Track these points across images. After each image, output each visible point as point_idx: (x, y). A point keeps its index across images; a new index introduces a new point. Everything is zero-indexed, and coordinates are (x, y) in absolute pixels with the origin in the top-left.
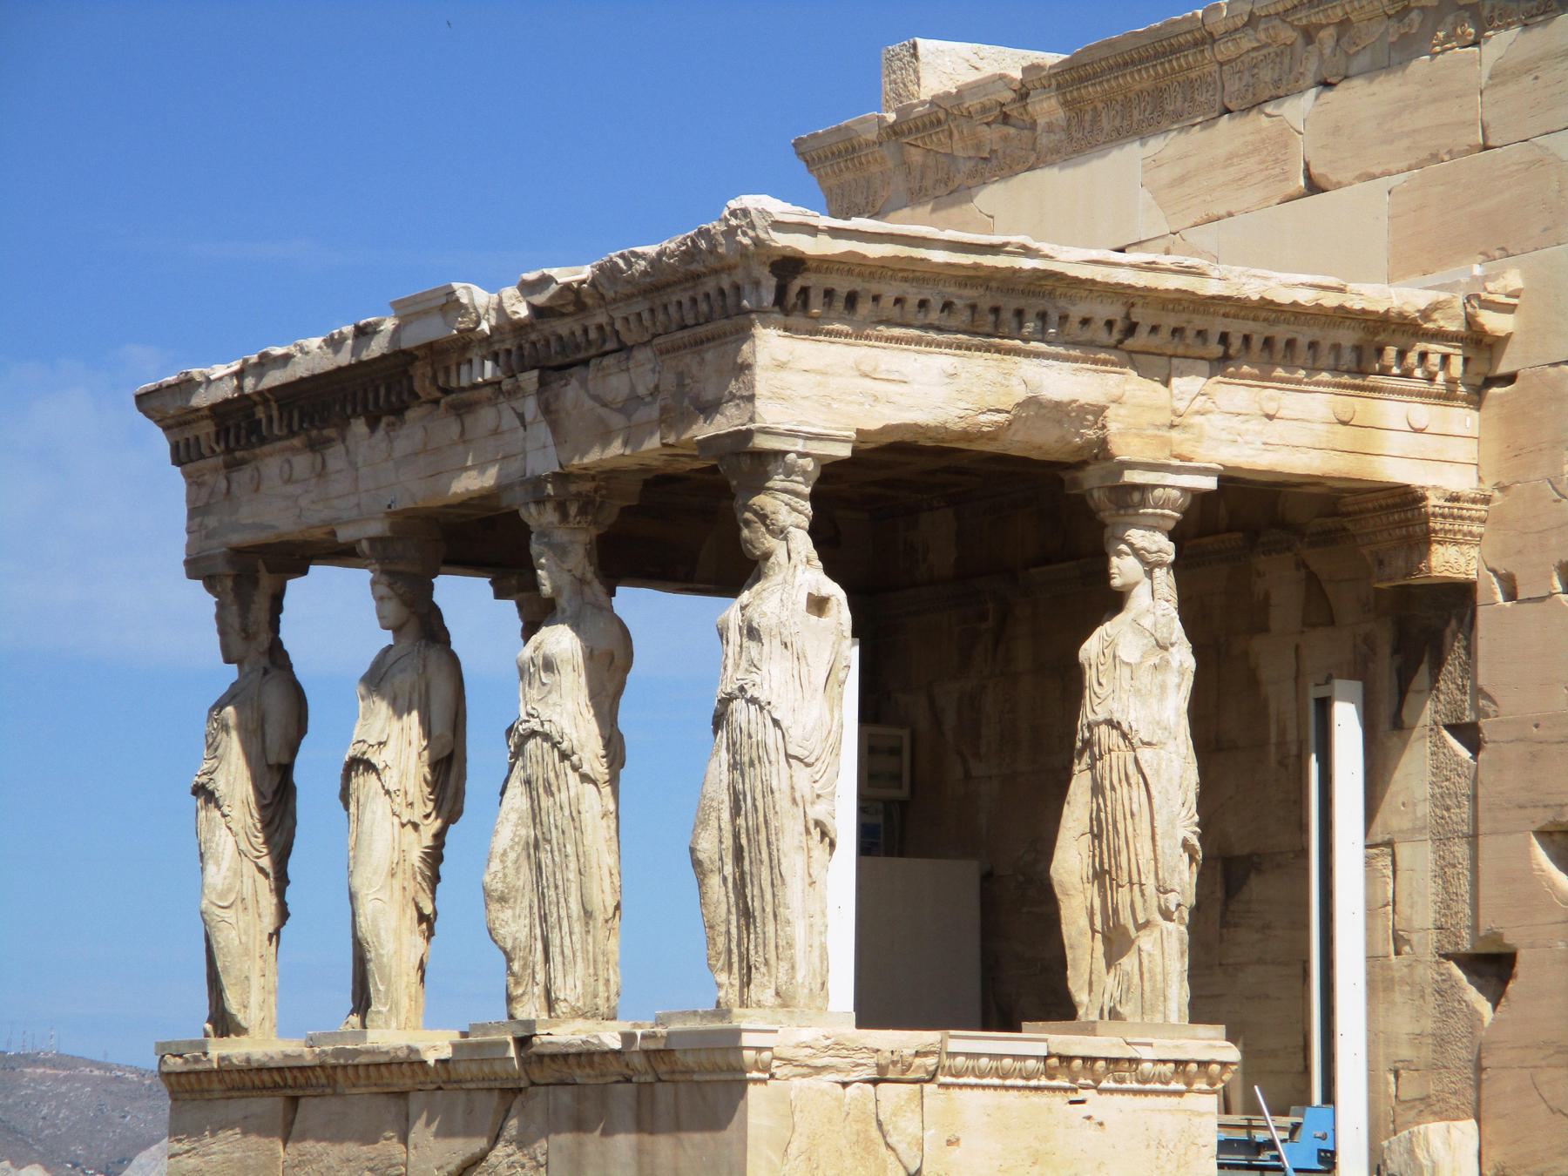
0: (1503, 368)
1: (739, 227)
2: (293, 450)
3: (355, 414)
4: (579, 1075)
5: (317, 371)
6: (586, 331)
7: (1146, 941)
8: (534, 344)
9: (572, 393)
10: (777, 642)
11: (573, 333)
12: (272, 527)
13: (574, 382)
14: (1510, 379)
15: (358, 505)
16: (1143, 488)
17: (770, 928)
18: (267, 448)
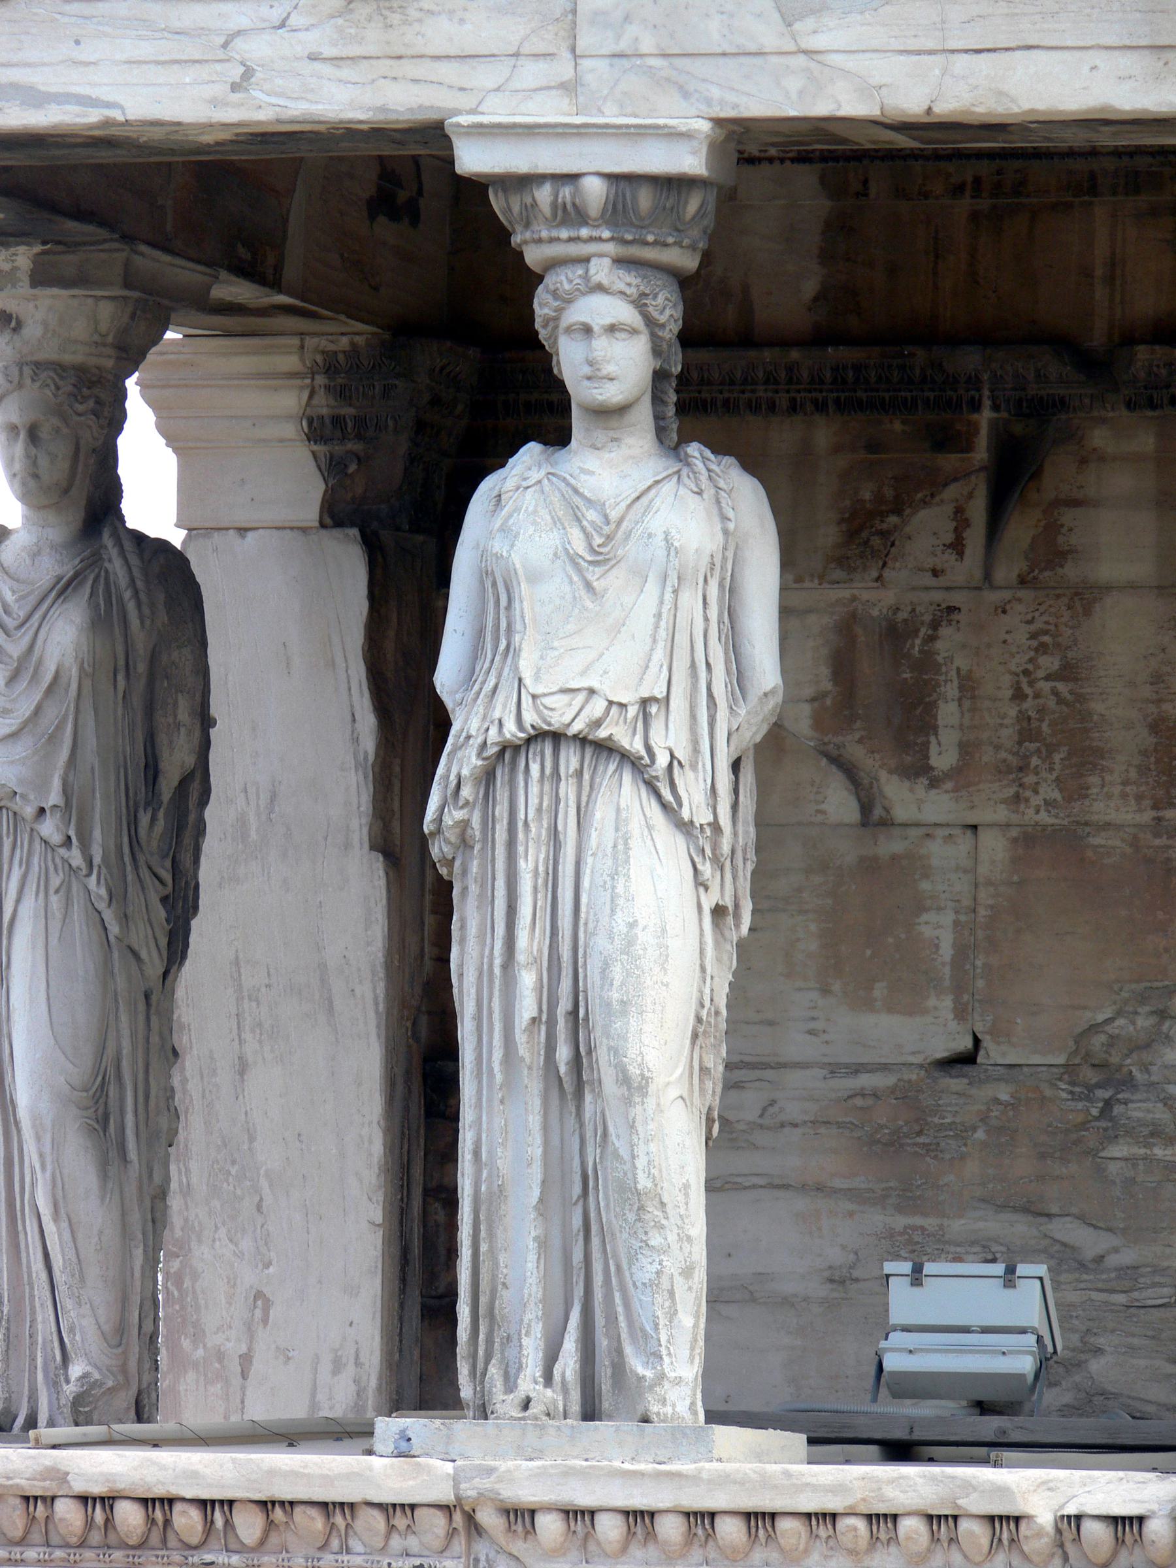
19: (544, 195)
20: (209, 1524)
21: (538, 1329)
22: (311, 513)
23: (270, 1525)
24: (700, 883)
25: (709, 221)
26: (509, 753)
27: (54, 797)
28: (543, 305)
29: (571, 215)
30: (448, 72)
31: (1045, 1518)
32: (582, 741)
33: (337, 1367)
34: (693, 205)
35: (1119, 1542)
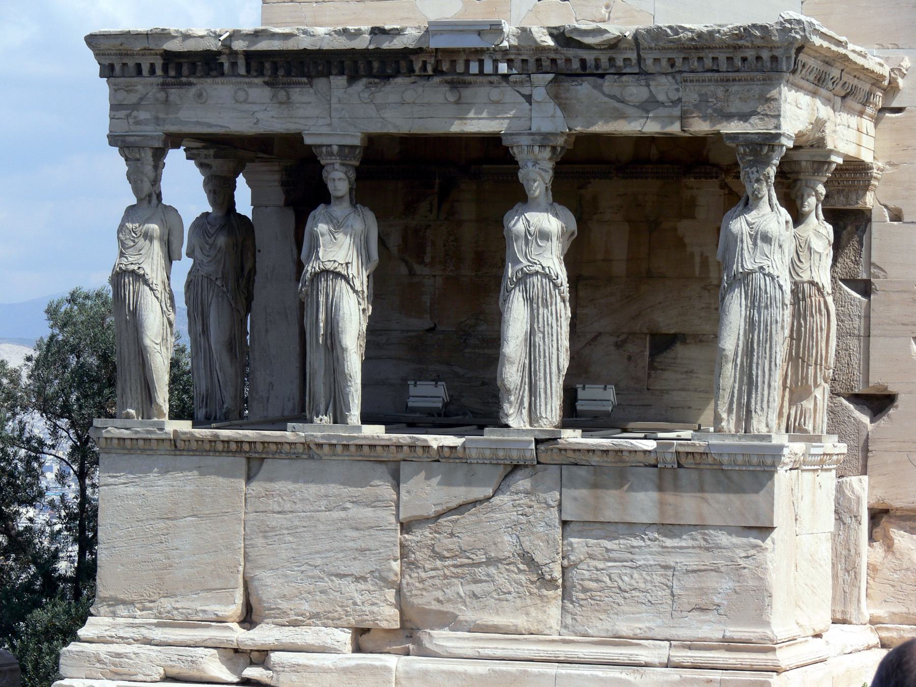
0: (895, 104)
1: (792, 29)
2: (250, 85)
3: (342, 73)
4: (595, 460)
5: (326, 47)
6: (611, 60)
7: (818, 393)
8: (554, 61)
9: (584, 89)
10: (777, 245)
11: (597, 60)
12: (224, 127)
13: (585, 84)
14: (899, 110)
15: (330, 125)
16: (830, 163)
17: (766, 393)
18: (219, 80)
19: (324, 149)
20: (250, 446)
21: (324, 403)
22: (282, 203)
23: (264, 447)
24: (359, 304)
25: (361, 155)
26: (317, 276)
27: (220, 276)
28: (324, 174)
29: (331, 154)
30: (302, 121)
31: (435, 447)
32: (333, 272)
33: (289, 400)
34: (357, 151)
35: (451, 452)
